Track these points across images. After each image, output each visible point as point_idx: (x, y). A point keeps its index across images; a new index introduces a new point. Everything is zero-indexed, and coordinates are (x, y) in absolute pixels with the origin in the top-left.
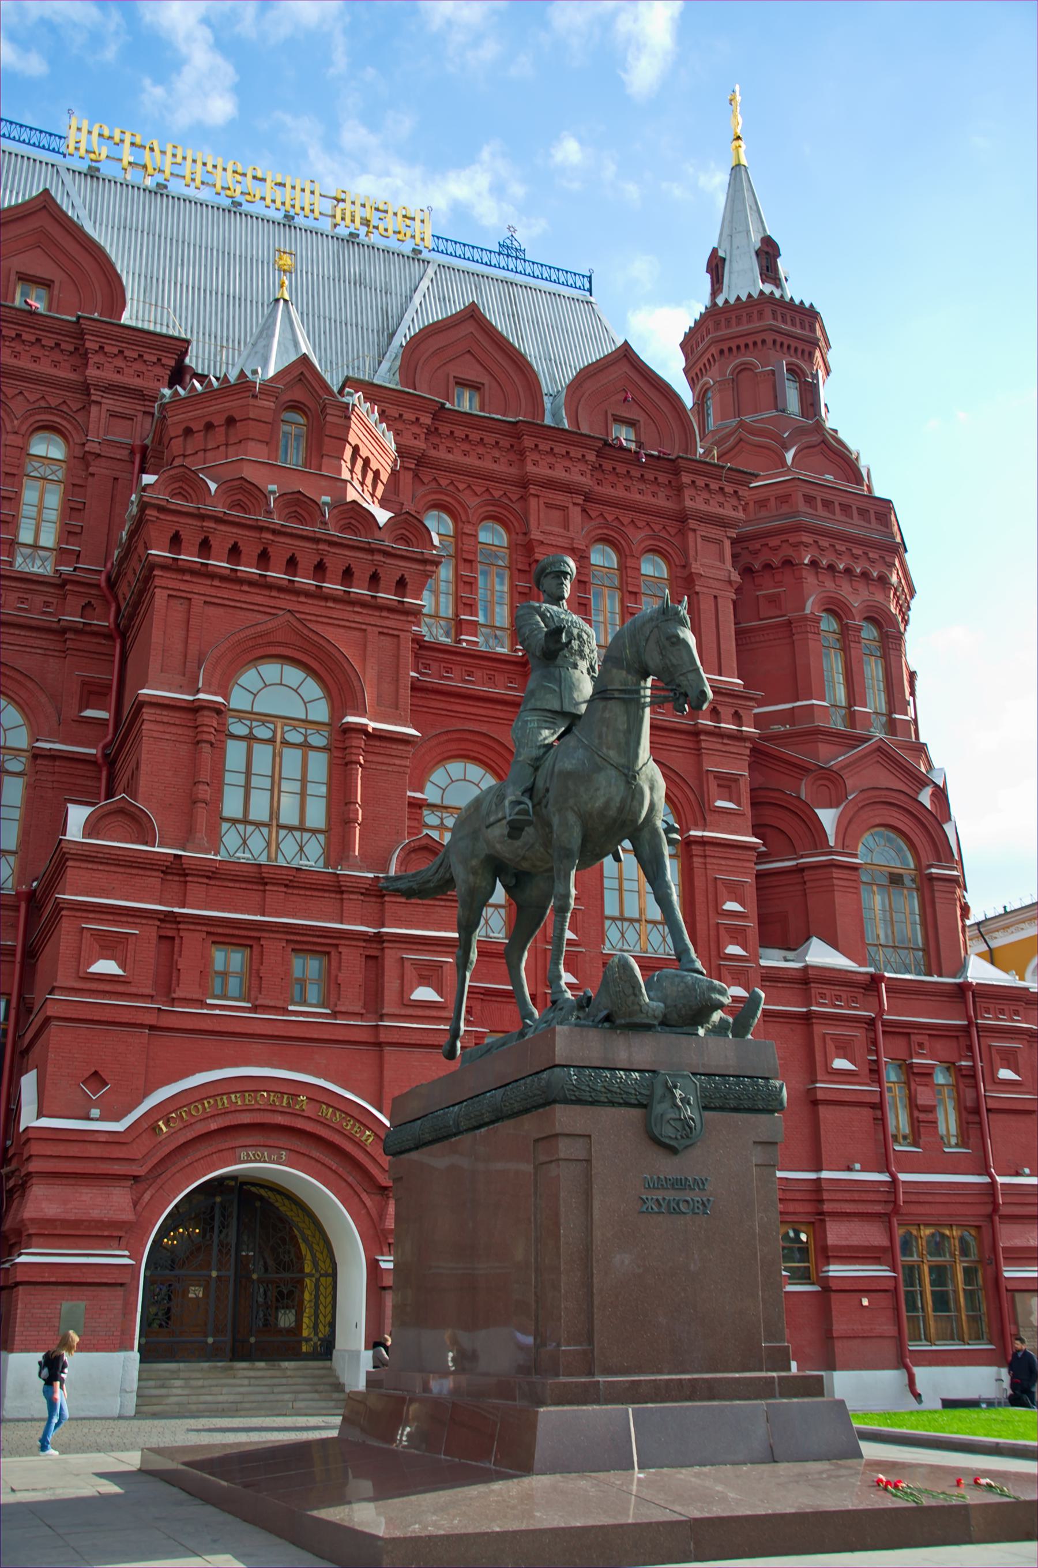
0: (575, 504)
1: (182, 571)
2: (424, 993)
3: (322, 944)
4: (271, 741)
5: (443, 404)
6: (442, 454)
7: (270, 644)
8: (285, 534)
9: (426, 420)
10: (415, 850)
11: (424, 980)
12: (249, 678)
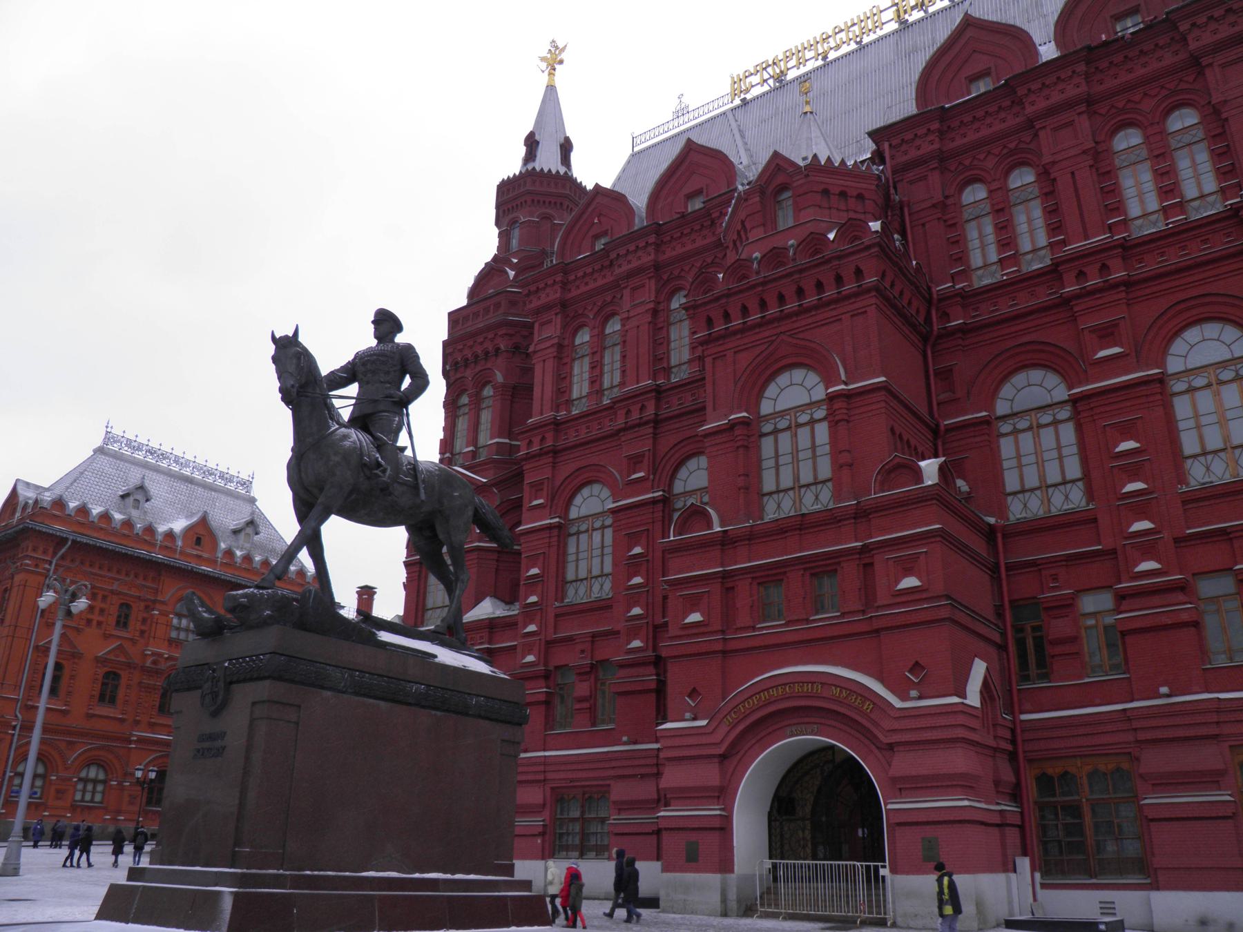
0: (1079, 114)
1: (717, 339)
2: (910, 582)
3: (825, 566)
4: (789, 428)
5: (943, 107)
6: (959, 142)
8: (770, 281)
9: (935, 125)
10: (890, 472)
11: (908, 572)
12: (772, 390)
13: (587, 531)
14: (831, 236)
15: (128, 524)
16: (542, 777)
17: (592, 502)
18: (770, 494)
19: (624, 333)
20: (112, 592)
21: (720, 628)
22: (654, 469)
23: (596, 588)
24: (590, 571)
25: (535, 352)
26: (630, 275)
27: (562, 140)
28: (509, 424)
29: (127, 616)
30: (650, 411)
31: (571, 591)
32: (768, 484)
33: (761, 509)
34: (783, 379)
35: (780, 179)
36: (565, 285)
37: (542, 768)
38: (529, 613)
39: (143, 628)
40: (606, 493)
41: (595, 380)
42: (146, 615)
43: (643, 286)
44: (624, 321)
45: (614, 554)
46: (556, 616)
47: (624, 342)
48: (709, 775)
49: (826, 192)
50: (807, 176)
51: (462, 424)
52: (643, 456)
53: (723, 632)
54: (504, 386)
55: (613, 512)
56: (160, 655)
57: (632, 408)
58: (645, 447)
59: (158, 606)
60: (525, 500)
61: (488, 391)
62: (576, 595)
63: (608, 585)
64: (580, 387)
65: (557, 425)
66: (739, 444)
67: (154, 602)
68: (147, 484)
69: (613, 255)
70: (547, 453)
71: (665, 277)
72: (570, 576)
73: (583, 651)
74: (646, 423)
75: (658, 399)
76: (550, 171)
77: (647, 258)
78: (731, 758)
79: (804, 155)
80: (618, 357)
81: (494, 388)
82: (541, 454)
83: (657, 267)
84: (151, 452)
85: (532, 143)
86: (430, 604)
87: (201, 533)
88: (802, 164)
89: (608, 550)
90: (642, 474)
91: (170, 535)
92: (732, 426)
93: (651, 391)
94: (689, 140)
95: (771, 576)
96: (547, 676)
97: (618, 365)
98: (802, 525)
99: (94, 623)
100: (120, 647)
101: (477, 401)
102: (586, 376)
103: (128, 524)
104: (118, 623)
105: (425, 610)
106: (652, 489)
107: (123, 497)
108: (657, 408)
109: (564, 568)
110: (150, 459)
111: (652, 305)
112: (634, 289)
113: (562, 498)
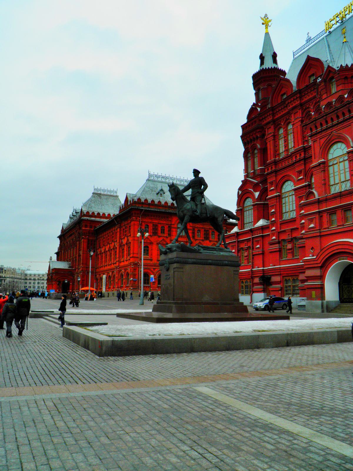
7: (331, 141)
12: (331, 151)
13: (288, 196)
14: (346, 96)
15: (159, 202)
16: (279, 273)
17: (289, 186)
18: (332, 185)
19: (293, 129)
21: (318, 228)
22: (305, 175)
23: (292, 214)
24: (289, 209)
25: (267, 139)
26: (293, 108)
27: (272, 54)
28: (263, 162)
29: (164, 230)
30: (303, 156)
31: (284, 216)
32: (332, 182)
33: (330, 190)
34: (335, 147)
35: (331, 75)
36: (274, 115)
37: (279, 271)
38: (273, 223)
40: (292, 184)
41: (286, 146)
43: (297, 112)
44: (293, 125)
45: (296, 203)
46: (281, 224)
47: (294, 132)
48: (317, 272)
50: (339, 74)
51: (250, 163)
52: (302, 171)
53: (320, 230)
54: (260, 149)
55: (295, 190)
57: (301, 153)
58: (302, 168)
60: (269, 188)
61: (256, 151)
62: (286, 217)
63: (295, 213)
64: (282, 149)
65: (276, 163)
66: (322, 170)
69: (287, 103)
70: (274, 172)
71: (304, 108)
72: (284, 211)
73: (289, 235)
74: (302, 159)
75: (305, 152)
76: (269, 68)
77: (298, 102)
78: (324, 266)
79: (337, 66)
80: (292, 137)
81: (257, 150)
82: (271, 173)
83: (301, 105)
84: (163, 177)
85: (262, 58)
86: (245, 222)
88: (337, 69)
89: (294, 202)
90: (302, 177)
92: (319, 164)
93: (302, 149)
94: (308, 57)
95: (332, 212)
96: (279, 243)
97: (292, 140)
98: (341, 195)
101: (253, 154)
102: (283, 145)
104: (162, 232)
105: (244, 224)
106: (305, 181)
107: (157, 194)
108: (305, 154)
109: (282, 209)
110: (163, 180)
111: (300, 119)
112: (295, 113)
113: (279, 186)
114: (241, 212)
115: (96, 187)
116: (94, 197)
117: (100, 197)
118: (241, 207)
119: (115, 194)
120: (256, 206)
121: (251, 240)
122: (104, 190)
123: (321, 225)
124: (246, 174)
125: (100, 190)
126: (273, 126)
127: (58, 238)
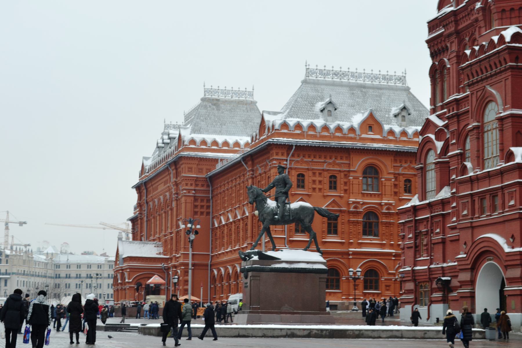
20: (323, 170)
29: (335, 182)
36: (457, 23)
39: (346, 188)
42: (346, 180)
49: (504, 11)
56: (358, 203)
59: (352, 174)
67: (349, 171)
68: (334, 100)
84: (336, 74)
87: (371, 123)
91: (352, 129)
99: (317, 189)
100: (334, 201)
103: (325, 128)
104: (331, 188)
105: (426, 193)
110: (336, 80)
114: (422, 173)
115: (208, 87)
116: (205, 107)
117: (218, 108)
118: (422, 164)
119: (249, 99)
120: (438, 166)
121: (430, 220)
122: (225, 92)
123: (473, 213)
124: (433, 107)
125: (217, 91)
126: (456, 39)
127: (134, 190)
